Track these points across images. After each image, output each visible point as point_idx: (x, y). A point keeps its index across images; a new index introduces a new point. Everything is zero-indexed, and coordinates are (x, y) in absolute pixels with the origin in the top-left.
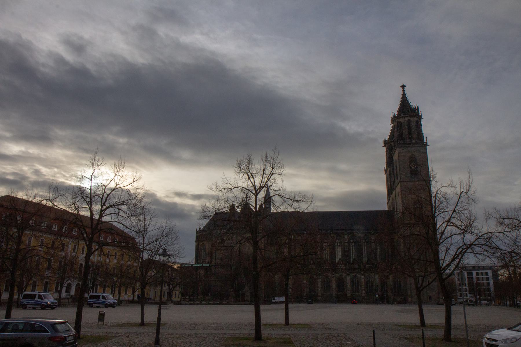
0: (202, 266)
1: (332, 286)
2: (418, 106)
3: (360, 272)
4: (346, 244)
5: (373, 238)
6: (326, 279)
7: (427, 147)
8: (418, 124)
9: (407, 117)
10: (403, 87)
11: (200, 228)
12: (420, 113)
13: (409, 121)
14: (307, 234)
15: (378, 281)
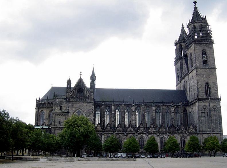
0: (43, 128)
3: (167, 134)
5: (173, 109)
7: (214, 44)
10: (195, 2)
11: (40, 99)
14: (125, 105)
15: (180, 140)
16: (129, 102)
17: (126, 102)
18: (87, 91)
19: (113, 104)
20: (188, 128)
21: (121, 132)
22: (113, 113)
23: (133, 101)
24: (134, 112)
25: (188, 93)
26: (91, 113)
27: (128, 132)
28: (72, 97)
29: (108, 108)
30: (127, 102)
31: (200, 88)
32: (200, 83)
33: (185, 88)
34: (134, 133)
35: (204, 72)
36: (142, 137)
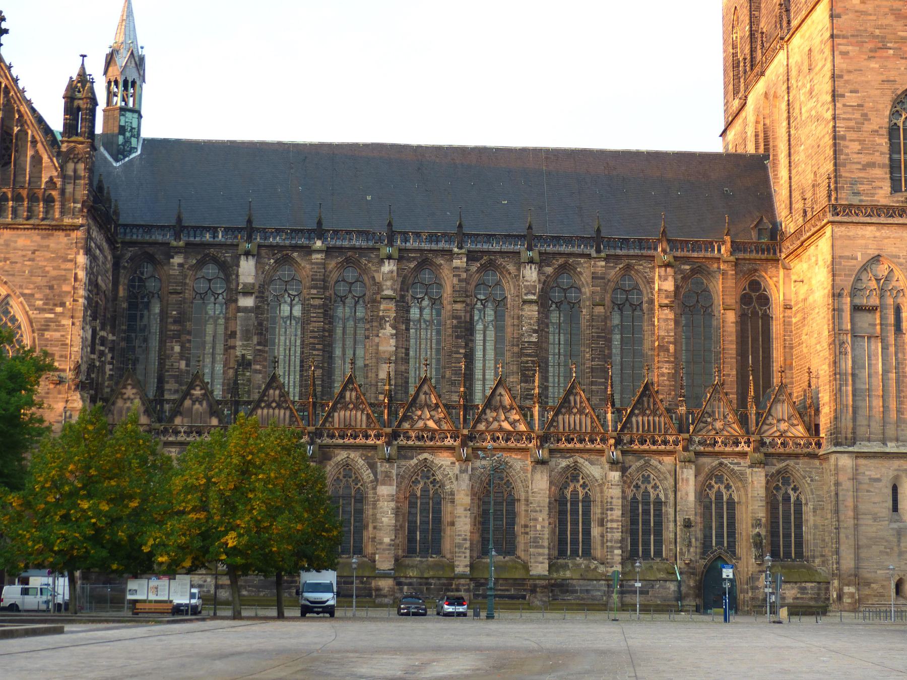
1: (452, 524)
3: (601, 452)
4: (526, 307)
6: (420, 486)
14: (329, 251)
15: (692, 497)
16: (360, 233)
17: (336, 232)
18: (39, 145)
19: (248, 246)
20: (758, 414)
22: (245, 310)
25: (783, 173)
26: (63, 305)
29: (211, 270)
30: (348, 232)
31: (850, 135)
32: (851, 99)
33: (766, 144)
34: (370, 442)
35: (890, 20)
36: (426, 470)
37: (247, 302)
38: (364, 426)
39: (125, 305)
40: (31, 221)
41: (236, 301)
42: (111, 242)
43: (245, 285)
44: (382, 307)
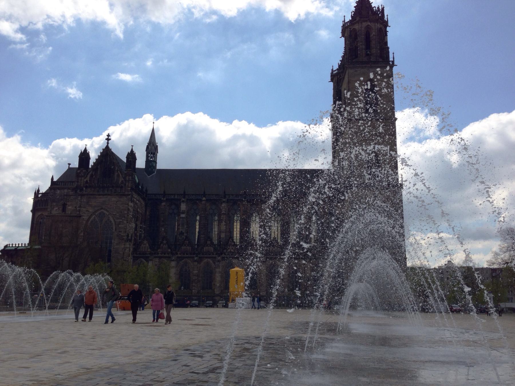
2: (384, 7)
8: (383, 34)
9: (367, 21)
12: (386, 17)
13: (368, 28)
14: (207, 200)
17: (209, 195)
19: (183, 199)
21: (187, 254)
22: (183, 218)
23: (225, 192)
24: (224, 214)
26: (125, 217)
27: (203, 254)
28: (88, 185)
29: (173, 207)
34: (214, 256)
37: (183, 216)
38: (213, 251)
39: (149, 217)
40: (116, 193)
41: (180, 215)
42: (144, 199)
43: (182, 211)
44: (222, 216)
